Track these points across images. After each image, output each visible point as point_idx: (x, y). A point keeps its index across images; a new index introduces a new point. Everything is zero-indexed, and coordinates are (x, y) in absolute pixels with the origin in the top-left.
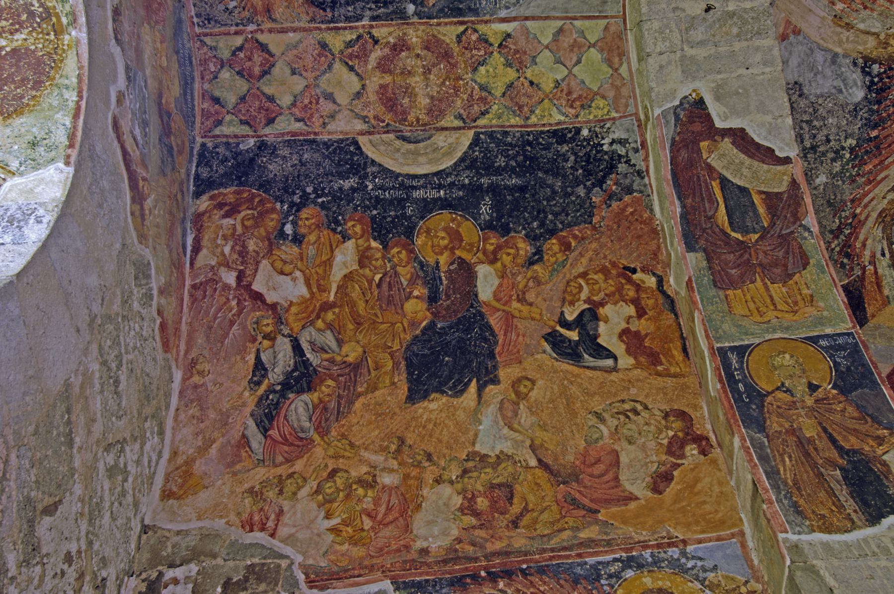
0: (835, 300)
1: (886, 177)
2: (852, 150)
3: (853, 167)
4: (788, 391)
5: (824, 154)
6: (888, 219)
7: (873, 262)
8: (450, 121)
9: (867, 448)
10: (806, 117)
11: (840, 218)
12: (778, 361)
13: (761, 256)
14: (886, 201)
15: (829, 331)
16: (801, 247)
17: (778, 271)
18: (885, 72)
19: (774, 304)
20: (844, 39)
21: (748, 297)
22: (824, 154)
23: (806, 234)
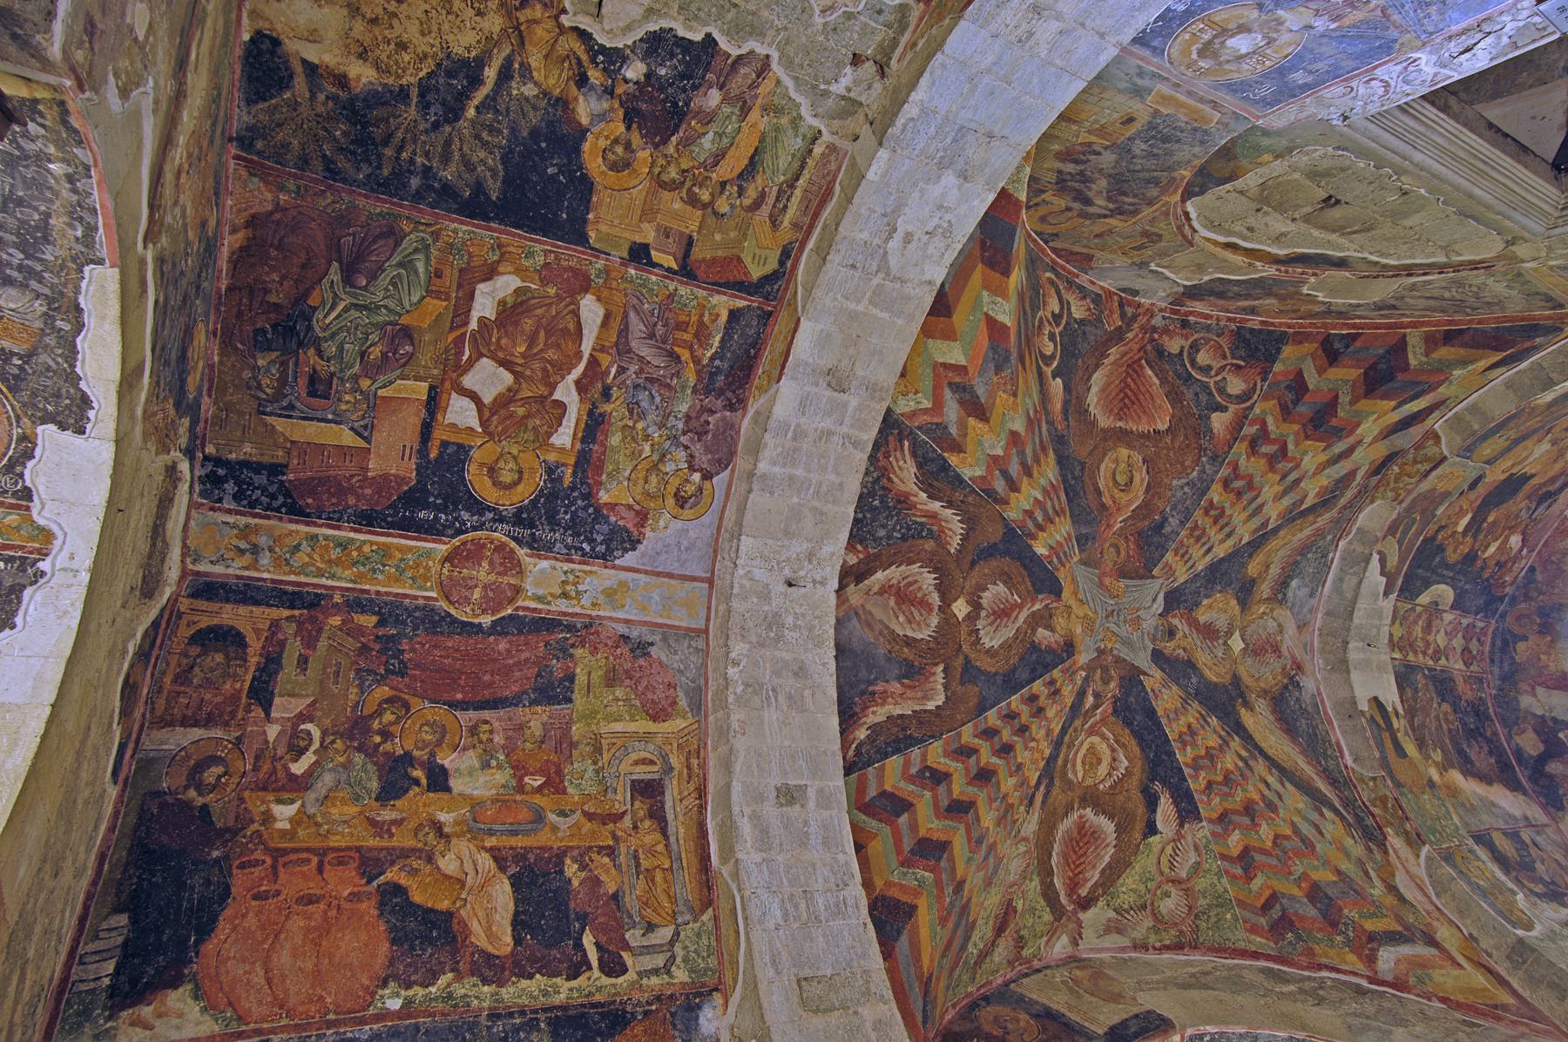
8: (1419, 609)
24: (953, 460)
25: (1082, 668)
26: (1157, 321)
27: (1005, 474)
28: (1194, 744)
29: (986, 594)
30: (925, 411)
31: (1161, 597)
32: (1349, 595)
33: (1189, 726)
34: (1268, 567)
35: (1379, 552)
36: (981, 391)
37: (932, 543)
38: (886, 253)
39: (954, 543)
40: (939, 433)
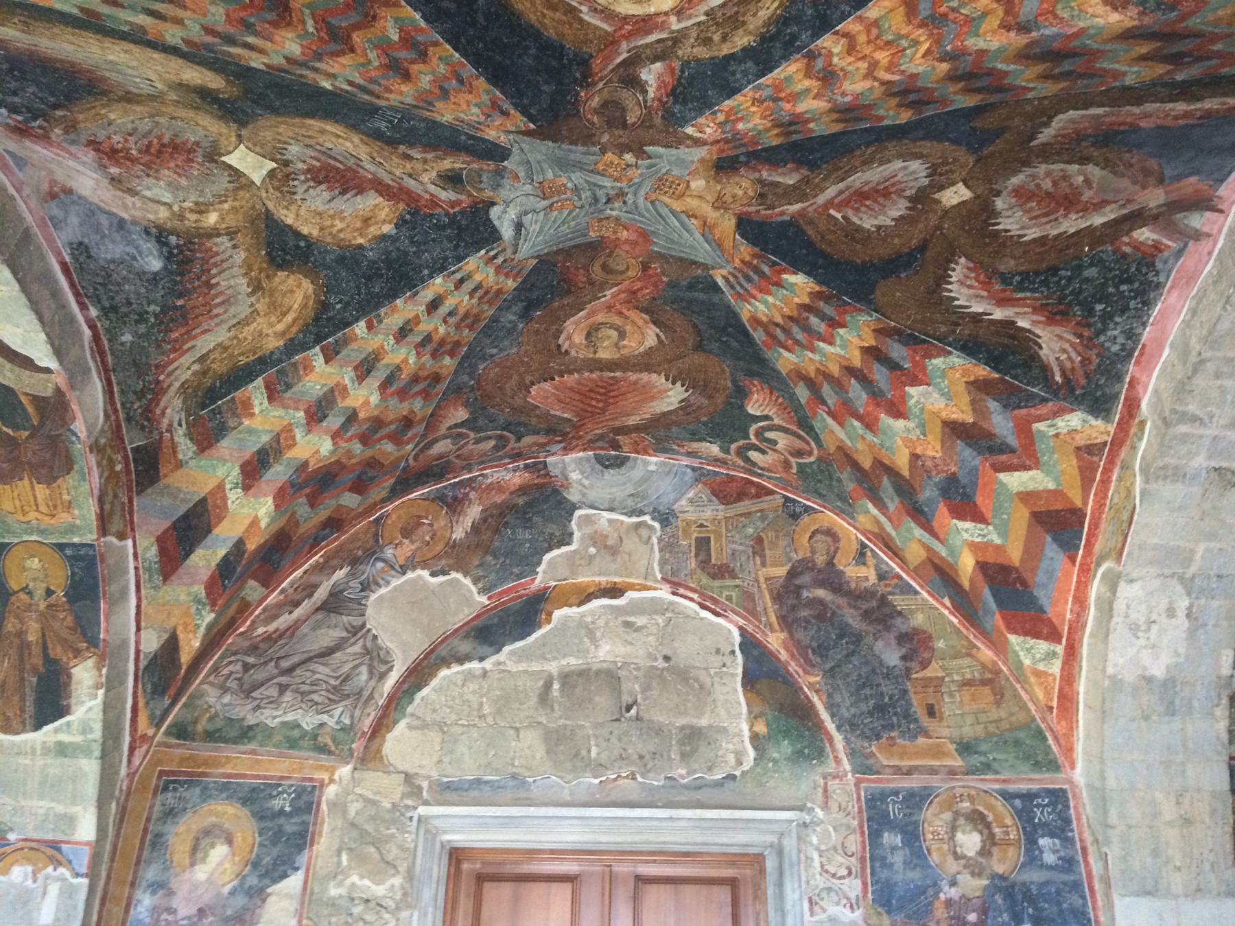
0: (89, 510)
1: (193, 347)
2: (156, 316)
3: (159, 332)
4: (30, 593)
5: (126, 315)
6: (190, 390)
7: (170, 430)
9: (65, 660)
10: (99, 280)
11: (144, 381)
12: (28, 563)
13: (30, 454)
14: (190, 372)
15: (76, 540)
16: (67, 451)
17: (44, 471)
18: (185, 244)
19: (37, 505)
20: (130, 205)
21: (16, 494)
22: (126, 315)
23: (74, 439)
24: (983, 371)
25: (698, 142)
26: (557, 447)
27: (894, 366)
28: (384, 47)
29: (896, 214)
30: (1040, 419)
31: (507, 232)
32: (35, 287)
33: (406, 76)
34: (257, 287)
35: (47, 371)
36: (968, 453)
37: (1002, 268)
38: (1189, 594)
39: (959, 270)
40: (1014, 399)
